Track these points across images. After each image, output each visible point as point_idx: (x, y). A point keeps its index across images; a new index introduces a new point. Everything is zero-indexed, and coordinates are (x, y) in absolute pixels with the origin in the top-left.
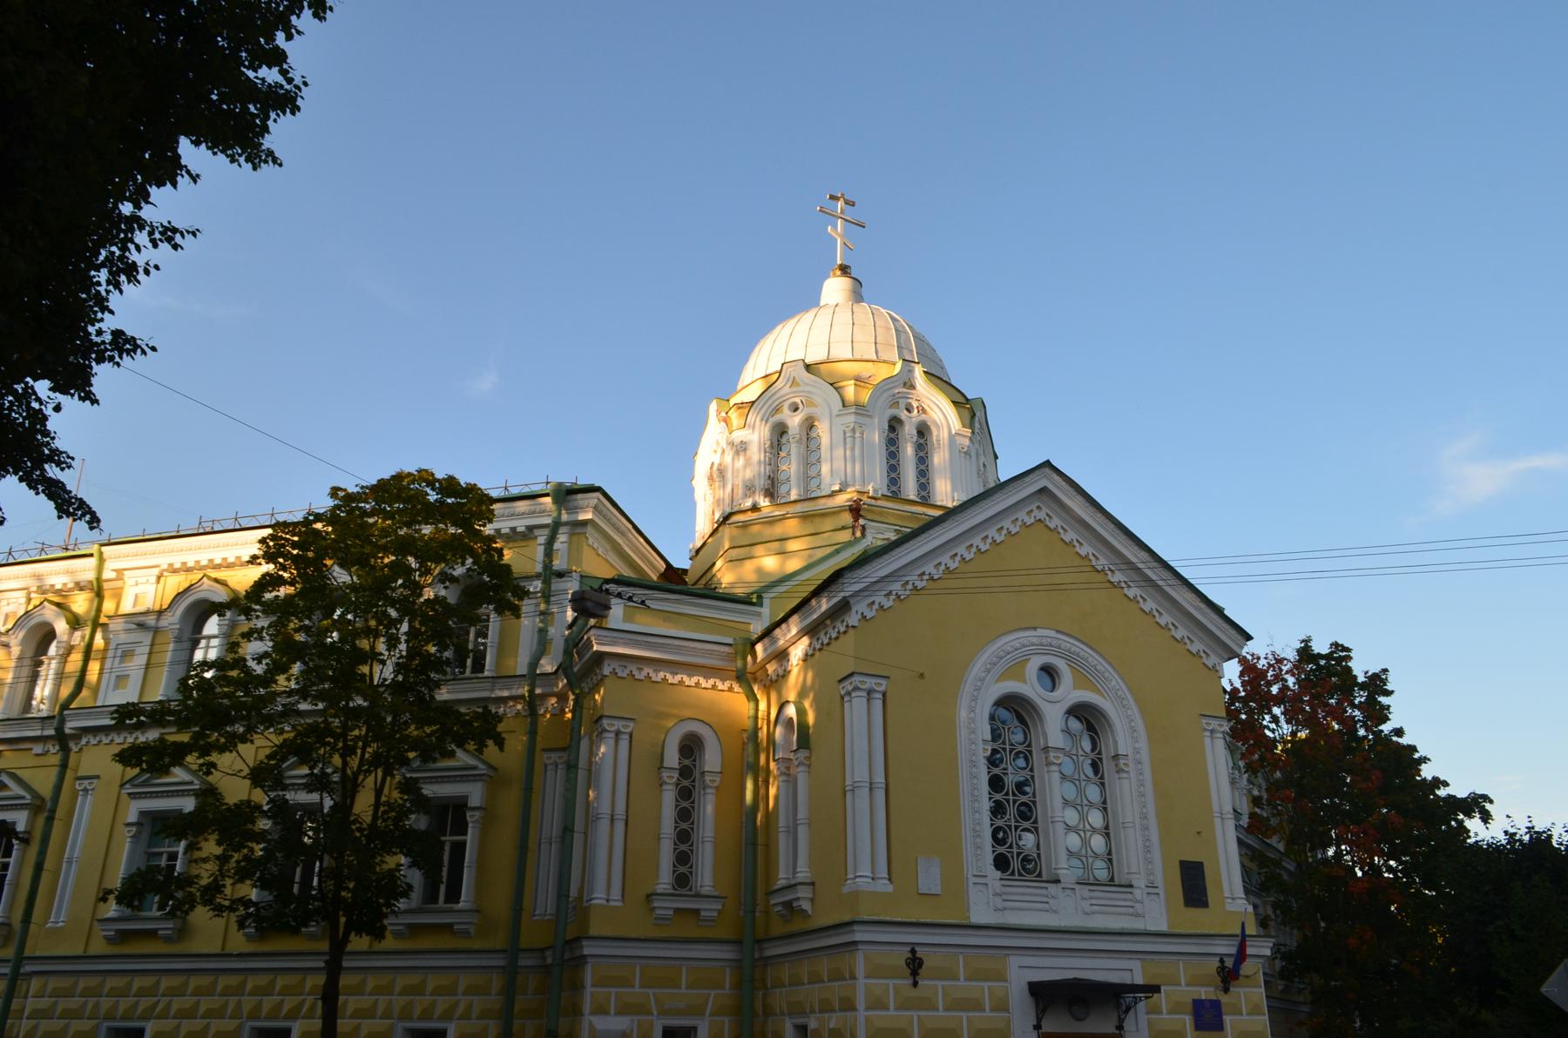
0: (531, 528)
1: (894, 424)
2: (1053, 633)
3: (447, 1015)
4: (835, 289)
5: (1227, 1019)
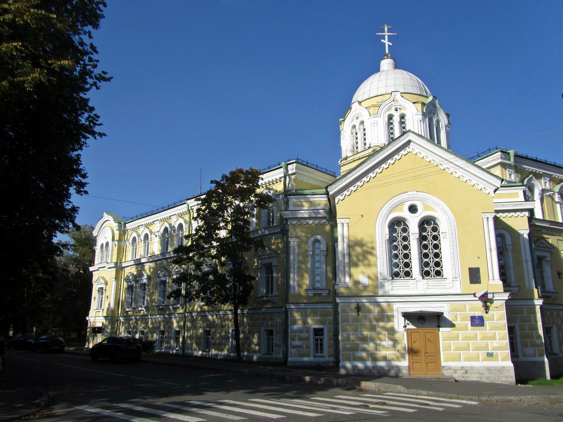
0: (281, 178)
1: (390, 117)
2: (415, 192)
3: (272, 326)
4: (386, 64)
5: (487, 323)
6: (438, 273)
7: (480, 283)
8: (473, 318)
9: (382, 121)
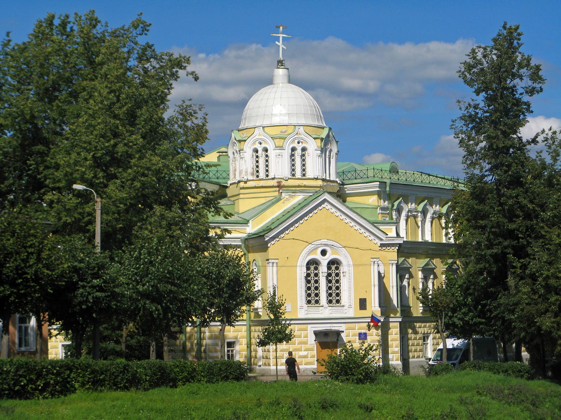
1: (293, 149)
2: (326, 240)
5: (368, 337)
6: (338, 301)
7: (366, 309)
8: (360, 334)
9: (287, 153)
